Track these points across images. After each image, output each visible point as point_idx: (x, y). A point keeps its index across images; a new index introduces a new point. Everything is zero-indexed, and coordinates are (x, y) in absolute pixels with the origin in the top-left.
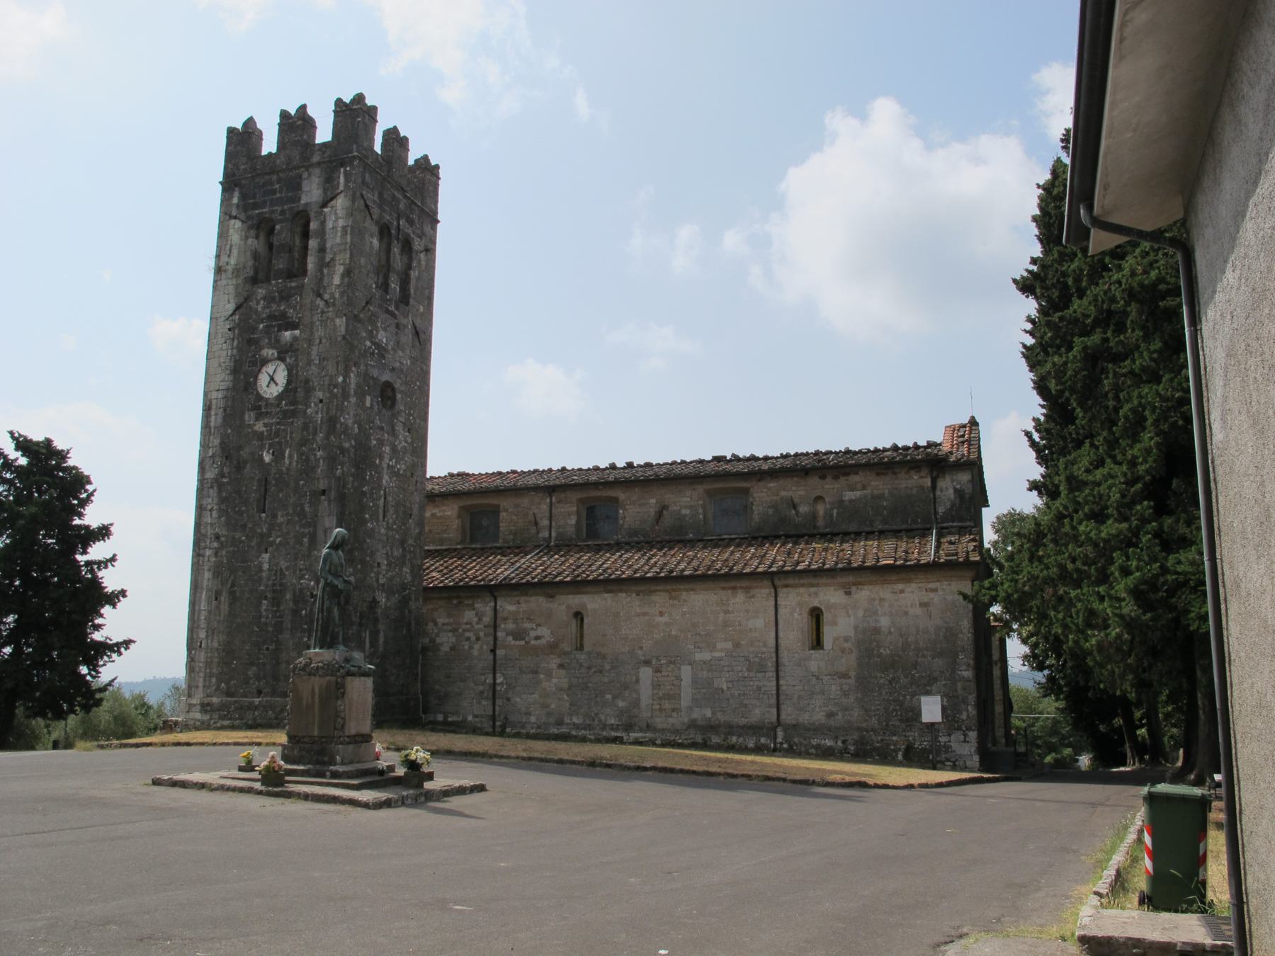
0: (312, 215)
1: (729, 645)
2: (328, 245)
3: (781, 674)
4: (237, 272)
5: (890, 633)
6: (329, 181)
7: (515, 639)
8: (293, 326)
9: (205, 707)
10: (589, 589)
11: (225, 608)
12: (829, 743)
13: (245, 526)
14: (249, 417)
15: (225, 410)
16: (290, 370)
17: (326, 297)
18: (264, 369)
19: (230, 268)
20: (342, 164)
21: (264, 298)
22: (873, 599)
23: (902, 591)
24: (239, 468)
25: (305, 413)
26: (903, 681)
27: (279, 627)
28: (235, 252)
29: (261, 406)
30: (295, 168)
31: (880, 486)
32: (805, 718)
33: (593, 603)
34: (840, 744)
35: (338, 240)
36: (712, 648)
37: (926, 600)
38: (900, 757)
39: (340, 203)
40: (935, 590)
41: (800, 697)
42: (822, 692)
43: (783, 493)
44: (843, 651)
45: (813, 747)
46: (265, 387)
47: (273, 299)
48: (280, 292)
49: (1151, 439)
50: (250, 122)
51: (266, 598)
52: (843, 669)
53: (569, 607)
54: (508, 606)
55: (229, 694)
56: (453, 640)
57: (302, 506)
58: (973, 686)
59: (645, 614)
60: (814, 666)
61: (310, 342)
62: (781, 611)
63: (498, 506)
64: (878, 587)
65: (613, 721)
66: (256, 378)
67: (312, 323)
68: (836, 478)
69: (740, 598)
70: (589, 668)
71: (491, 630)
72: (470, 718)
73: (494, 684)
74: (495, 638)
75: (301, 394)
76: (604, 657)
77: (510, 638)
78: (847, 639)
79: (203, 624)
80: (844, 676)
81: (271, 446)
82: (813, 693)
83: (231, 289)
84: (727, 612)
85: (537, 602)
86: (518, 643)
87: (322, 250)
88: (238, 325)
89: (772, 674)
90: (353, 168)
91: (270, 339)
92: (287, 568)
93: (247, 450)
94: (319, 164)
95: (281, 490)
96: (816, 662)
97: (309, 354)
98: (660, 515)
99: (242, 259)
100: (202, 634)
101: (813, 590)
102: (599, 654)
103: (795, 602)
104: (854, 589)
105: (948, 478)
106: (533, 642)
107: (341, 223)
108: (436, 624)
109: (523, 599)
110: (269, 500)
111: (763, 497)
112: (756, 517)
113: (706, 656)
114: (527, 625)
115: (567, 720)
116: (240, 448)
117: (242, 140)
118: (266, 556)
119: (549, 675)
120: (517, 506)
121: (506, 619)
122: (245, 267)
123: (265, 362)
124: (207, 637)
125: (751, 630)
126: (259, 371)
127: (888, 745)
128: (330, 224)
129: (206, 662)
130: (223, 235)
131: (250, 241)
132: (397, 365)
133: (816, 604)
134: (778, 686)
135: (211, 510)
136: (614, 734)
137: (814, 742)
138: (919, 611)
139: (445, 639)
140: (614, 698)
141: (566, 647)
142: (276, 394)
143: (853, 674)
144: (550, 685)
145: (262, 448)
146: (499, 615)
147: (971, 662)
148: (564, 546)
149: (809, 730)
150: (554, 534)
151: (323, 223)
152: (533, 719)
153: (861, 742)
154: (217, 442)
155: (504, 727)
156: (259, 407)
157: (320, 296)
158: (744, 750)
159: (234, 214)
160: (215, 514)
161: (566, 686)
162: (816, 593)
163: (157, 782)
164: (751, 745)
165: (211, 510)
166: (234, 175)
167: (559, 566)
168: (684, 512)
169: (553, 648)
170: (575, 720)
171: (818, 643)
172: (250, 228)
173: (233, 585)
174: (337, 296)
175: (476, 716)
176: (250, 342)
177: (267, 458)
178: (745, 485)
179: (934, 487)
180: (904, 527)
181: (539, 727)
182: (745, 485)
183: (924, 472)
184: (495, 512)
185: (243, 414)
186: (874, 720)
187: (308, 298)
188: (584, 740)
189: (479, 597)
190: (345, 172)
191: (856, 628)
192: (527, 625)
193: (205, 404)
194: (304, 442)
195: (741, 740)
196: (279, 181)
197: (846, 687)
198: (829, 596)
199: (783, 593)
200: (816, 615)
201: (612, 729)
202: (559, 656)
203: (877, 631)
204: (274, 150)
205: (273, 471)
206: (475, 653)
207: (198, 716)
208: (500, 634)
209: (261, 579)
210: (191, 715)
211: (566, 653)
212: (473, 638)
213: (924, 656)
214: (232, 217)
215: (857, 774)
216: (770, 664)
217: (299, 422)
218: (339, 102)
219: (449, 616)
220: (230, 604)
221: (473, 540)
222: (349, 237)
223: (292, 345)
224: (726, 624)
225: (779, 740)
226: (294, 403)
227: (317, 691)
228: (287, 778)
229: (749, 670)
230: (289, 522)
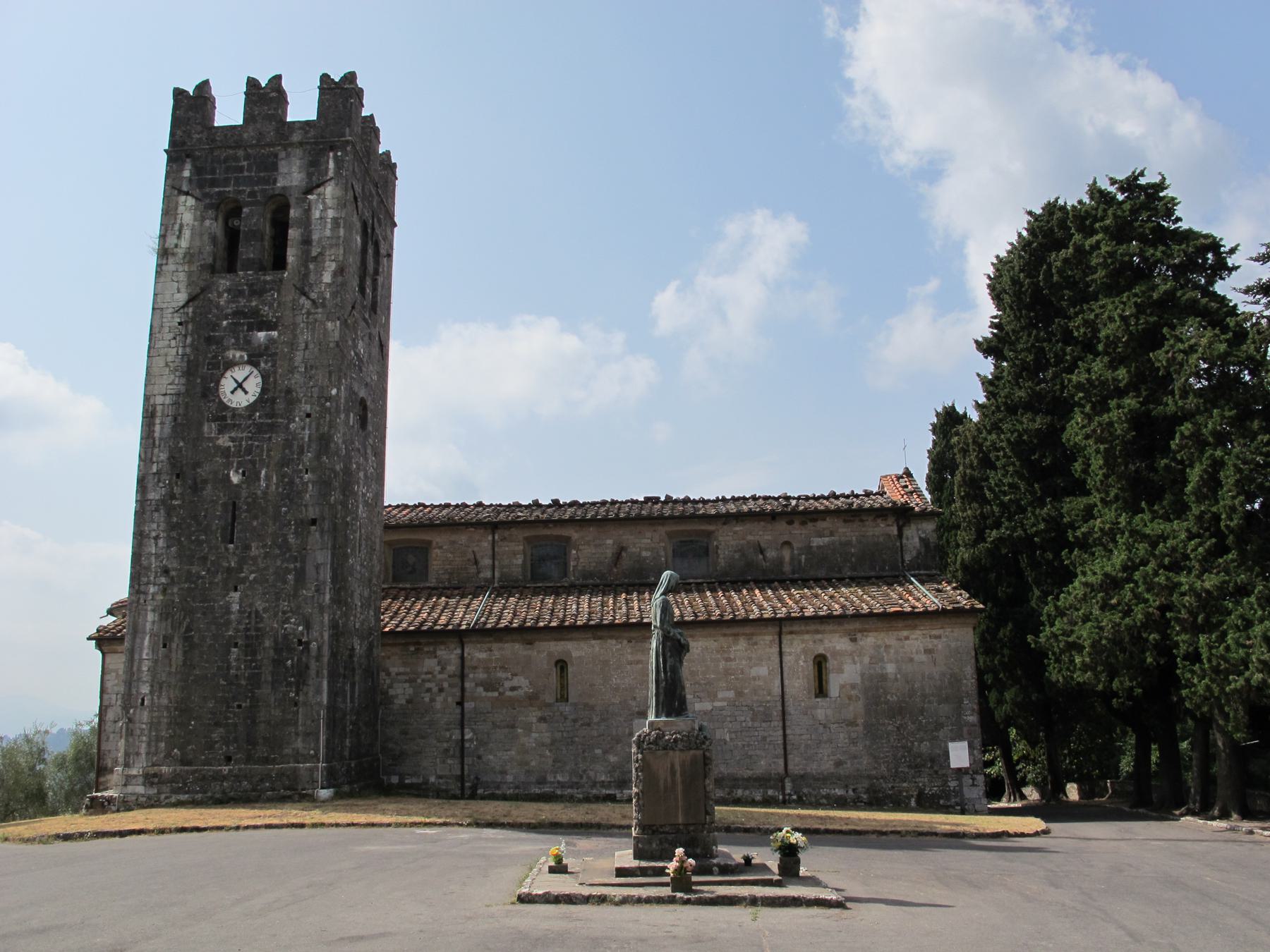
0: (292, 201)
1: (731, 694)
2: (315, 237)
3: (788, 723)
4: (190, 256)
5: (896, 679)
6: (314, 168)
7: (486, 690)
8: (268, 326)
9: (149, 779)
10: (575, 635)
11: (178, 657)
12: (839, 792)
13: (205, 559)
14: (209, 429)
15: (175, 419)
16: (265, 377)
17: (313, 296)
18: (228, 374)
19: (180, 252)
20: (332, 148)
21: (229, 291)
22: (879, 647)
23: (907, 638)
24: (196, 488)
25: (287, 428)
26: (911, 727)
27: (255, 680)
28: (187, 233)
29: (225, 418)
30: (269, 145)
31: (847, 532)
32: (813, 768)
33: (577, 650)
34: (851, 792)
35: (328, 233)
36: (713, 697)
37: (930, 646)
38: (913, 803)
39: (329, 190)
40: (939, 637)
41: (807, 746)
42: (830, 741)
43: (750, 538)
44: (850, 698)
45: (823, 797)
46: (228, 394)
47: (241, 293)
48: (251, 286)
49: (1234, 498)
50: (204, 87)
51: (236, 645)
52: (850, 716)
53: (550, 655)
54: (477, 653)
55: (184, 762)
56: (411, 691)
57: (285, 536)
58: (978, 730)
59: (638, 662)
60: (820, 714)
61: (292, 345)
62: (786, 659)
63: (430, 543)
64: (883, 634)
65: (603, 778)
66: (218, 383)
67: (295, 325)
68: (803, 523)
69: (742, 644)
70: (575, 721)
71: (457, 680)
72: (432, 779)
73: (463, 740)
74: (463, 689)
75: (280, 406)
76: (592, 708)
77: (481, 689)
78: (853, 686)
79: (145, 676)
80: (852, 723)
81: (240, 465)
82: (821, 742)
83: (182, 276)
84: (728, 660)
85: (514, 649)
86: (490, 694)
87: (306, 242)
88: (193, 320)
89: (777, 723)
90: (345, 153)
91: (237, 339)
92: (265, 610)
93: (207, 467)
94: (301, 144)
95: (256, 517)
96: (823, 709)
97: (291, 359)
98: (618, 557)
99: (197, 243)
100: (145, 689)
101: (819, 636)
102: (586, 705)
103: (799, 649)
104: (859, 636)
105: (913, 527)
106: (509, 693)
107: (331, 214)
108: (388, 674)
109: (495, 646)
110: (238, 527)
111: (728, 542)
112: (722, 562)
113: (707, 706)
114: (501, 675)
115: (550, 778)
116: (197, 465)
117: (192, 107)
118: (236, 596)
119: (528, 729)
120: (453, 542)
121: (475, 668)
122: (200, 252)
123: (230, 365)
124: (152, 692)
125: (754, 679)
126: (222, 375)
127: (900, 792)
128: (316, 214)
129: (151, 723)
130: (169, 212)
131: (207, 223)
132: (369, 380)
133: (821, 650)
134: (785, 736)
135: (156, 538)
136: (605, 792)
137: (824, 792)
138: (923, 657)
139: (399, 691)
140: (606, 752)
141: (549, 698)
142: (245, 404)
143: (860, 721)
144: (530, 741)
145: (228, 466)
146: (467, 663)
147: (975, 707)
148: (506, 588)
149: (818, 779)
150: (497, 574)
151: (308, 211)
152: (509, 778)
153: (872, 790)
154: (163, 456)
155: (474, 788)
156: (224, 418)
157: (305, 294)
158: (754, 803)
159: (185, 188)
160: (161, 543)
161: (548, 741)
162: (821, 641)
163: (524, 899)
164: (758, 798)
165: (156, 538)
166: (184, 143)
167: (510, 610)
168: (644, 554)
169: (532, 699)
170: (559, 778)
171: (821, 691)
172: (207, 207)
173: (189, 629)
174: (328, 296)
175: (440, 777)
176: (209, 340)
177: (235, 479)
178: (711, 528)
179: (900, 535)
180: (873, 574)
181: (517, 787)
182: (711, 528)
183: (891, 520)
184: (424, 550)
185: (201, 425)
186: (883, 768)
187: (289, 295)
188: (571, 799)
189: (442, 643)
190: (336, 157)
191: (862, 675)
192: (501, 675)
193: (145, 410)
194: (285, 462)
195: (747, 792)
196: (247, 157)
197: (854, 735)
198: (835, 643)
199: (786, 639)
200: (820, 663)
201: (603, 786)
202: (540, 709)
203: (883, 677)
204: (239, 120)
205: (244, 493)
206: (438, 705)
207: (140, 789)
208: (467, 685)
209: (228, 623)
210: (130, 789)
211: (549, 705)
212: (435, 689)
213: (930, 702)
214: (181, 192)
215: (957, 825)
216: (776, 713)
217: (278, 439)
218: (325, 78)
219: (405, 664)
220: (185, 653)
221: (396, 579)
222: (342, 232)
223: (267, 348)
224: (727, 672)
225: (788, 791)
226: (272, 415)
227: (678, 768)
228: (694, 879)
229: (753, 720)
230: (266, 555)
